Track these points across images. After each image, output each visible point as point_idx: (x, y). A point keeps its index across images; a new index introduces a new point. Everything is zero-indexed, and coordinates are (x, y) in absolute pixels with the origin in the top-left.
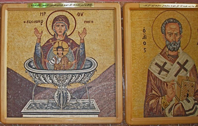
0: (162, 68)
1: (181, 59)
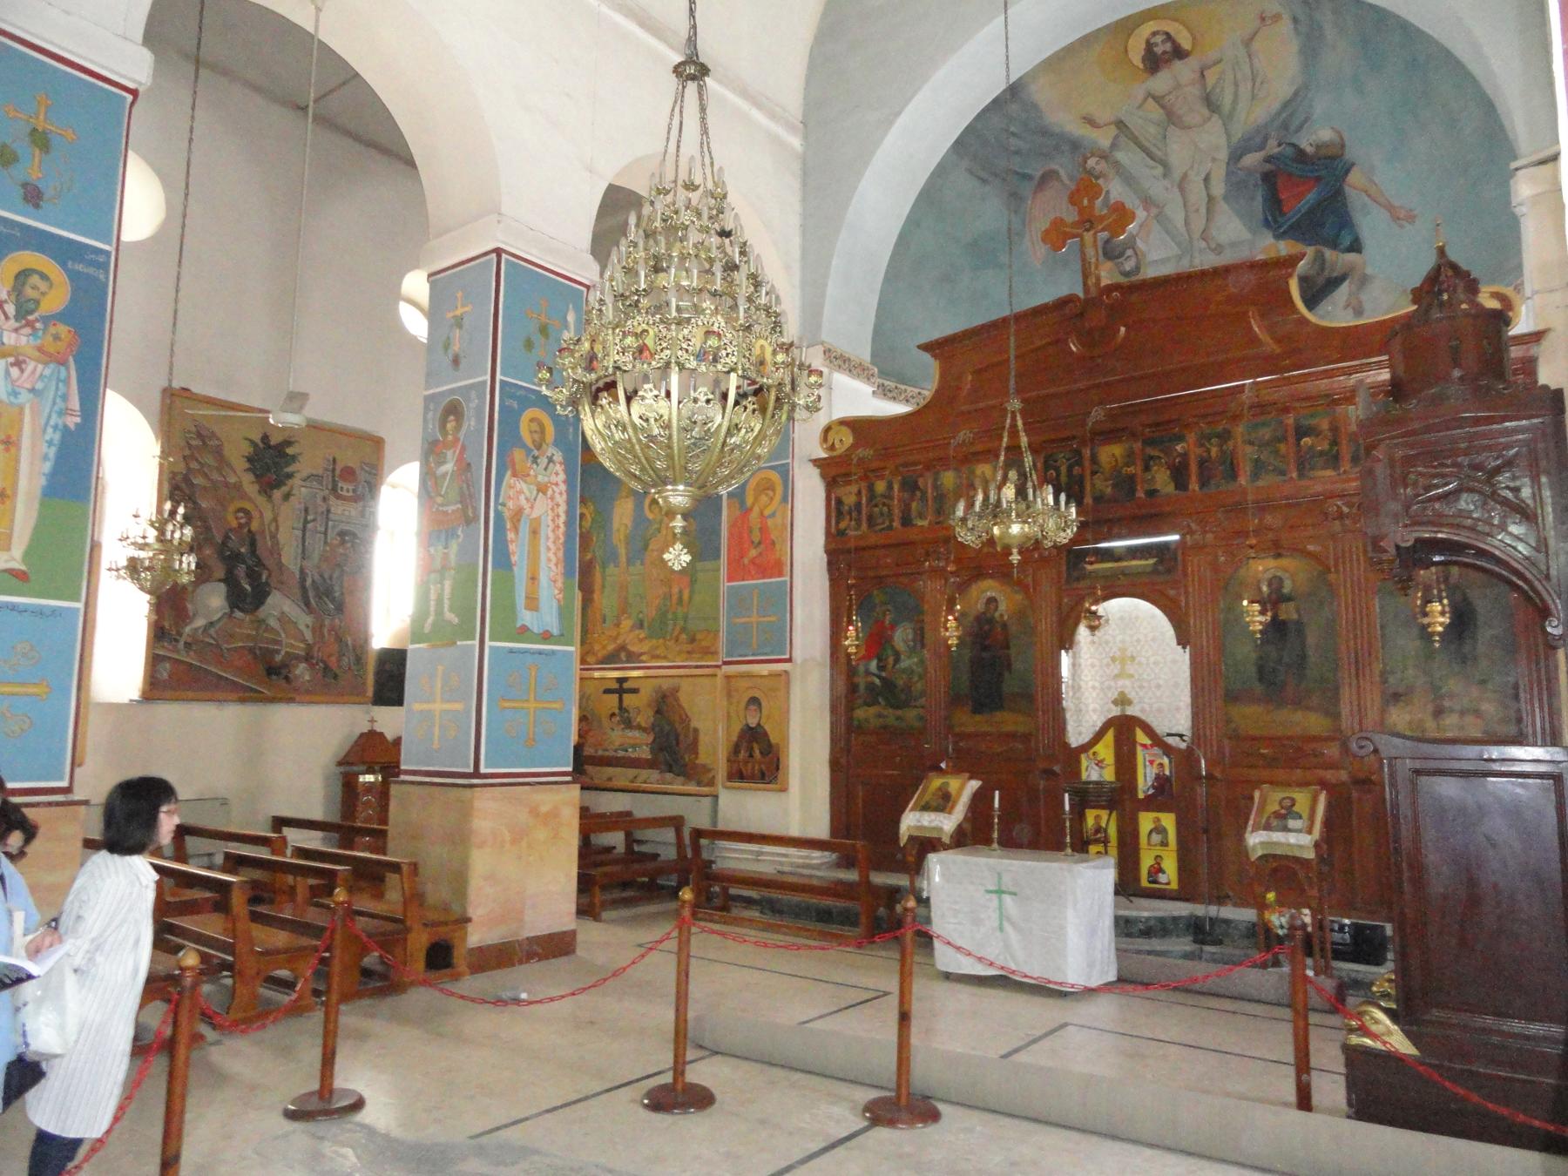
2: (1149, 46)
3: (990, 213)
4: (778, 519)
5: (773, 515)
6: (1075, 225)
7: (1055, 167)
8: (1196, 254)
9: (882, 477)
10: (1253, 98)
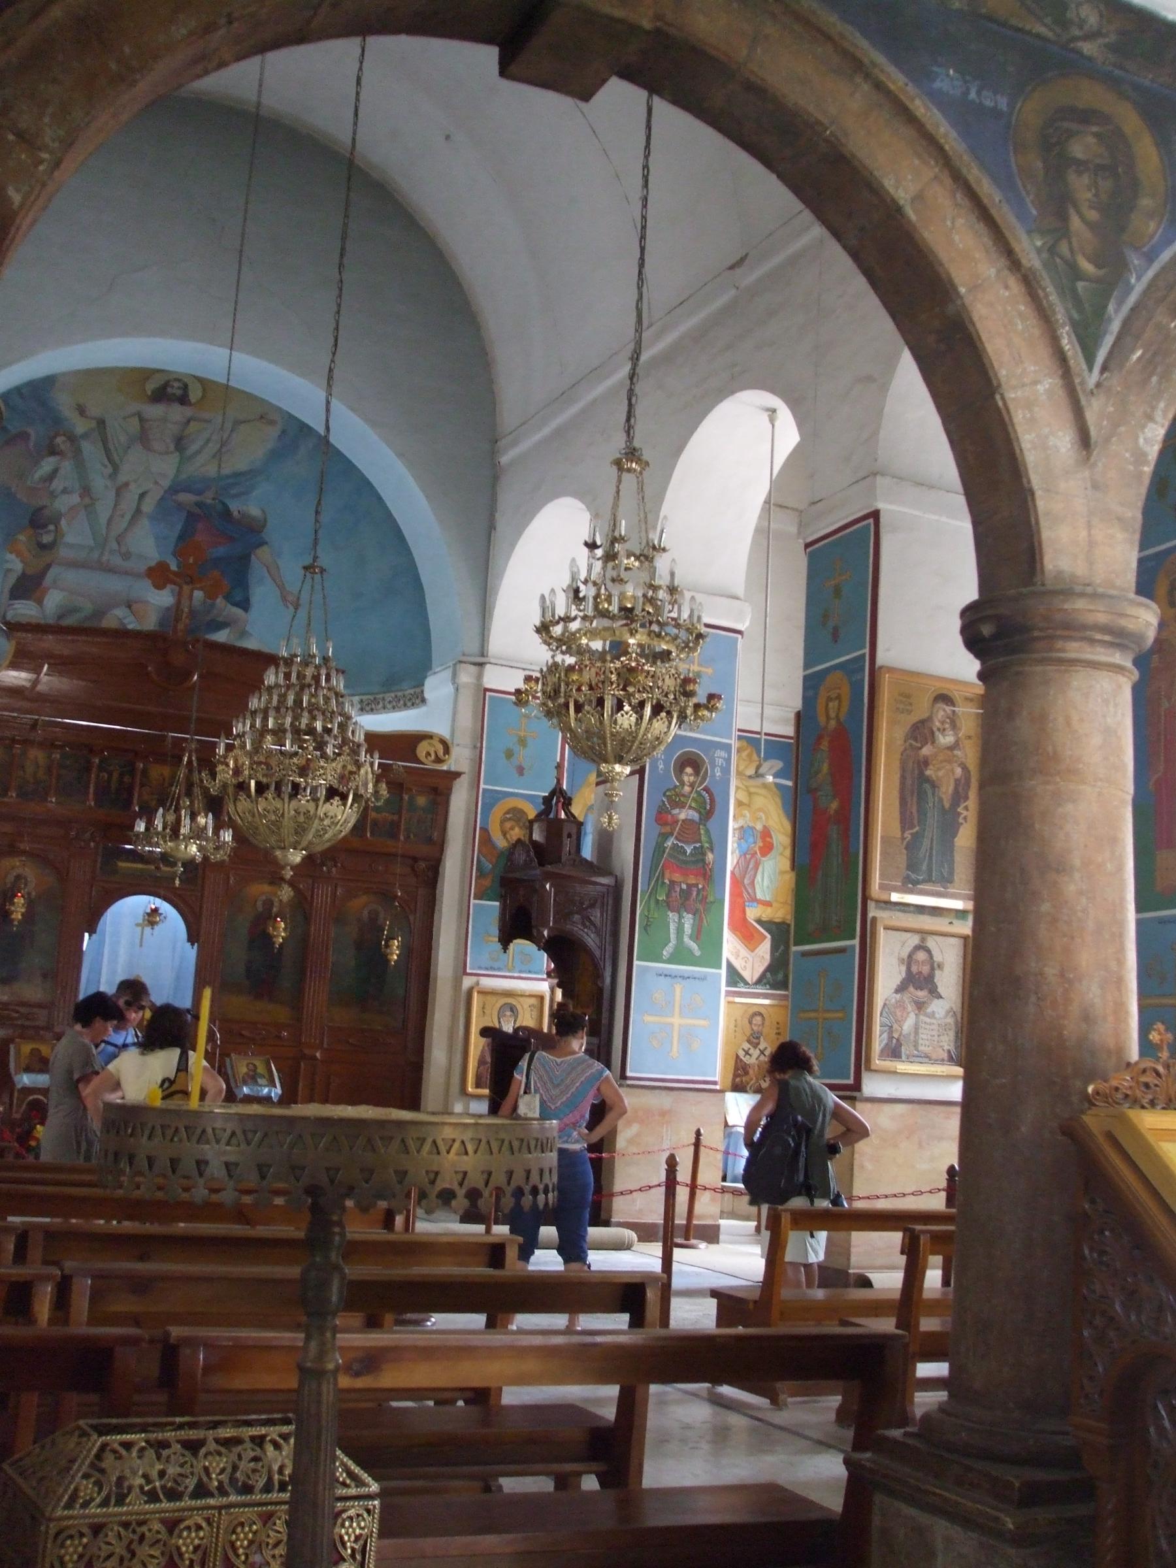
0: (747, 1053)
1: (762, 1047)
2: (166, 385)
6: (175, 573)
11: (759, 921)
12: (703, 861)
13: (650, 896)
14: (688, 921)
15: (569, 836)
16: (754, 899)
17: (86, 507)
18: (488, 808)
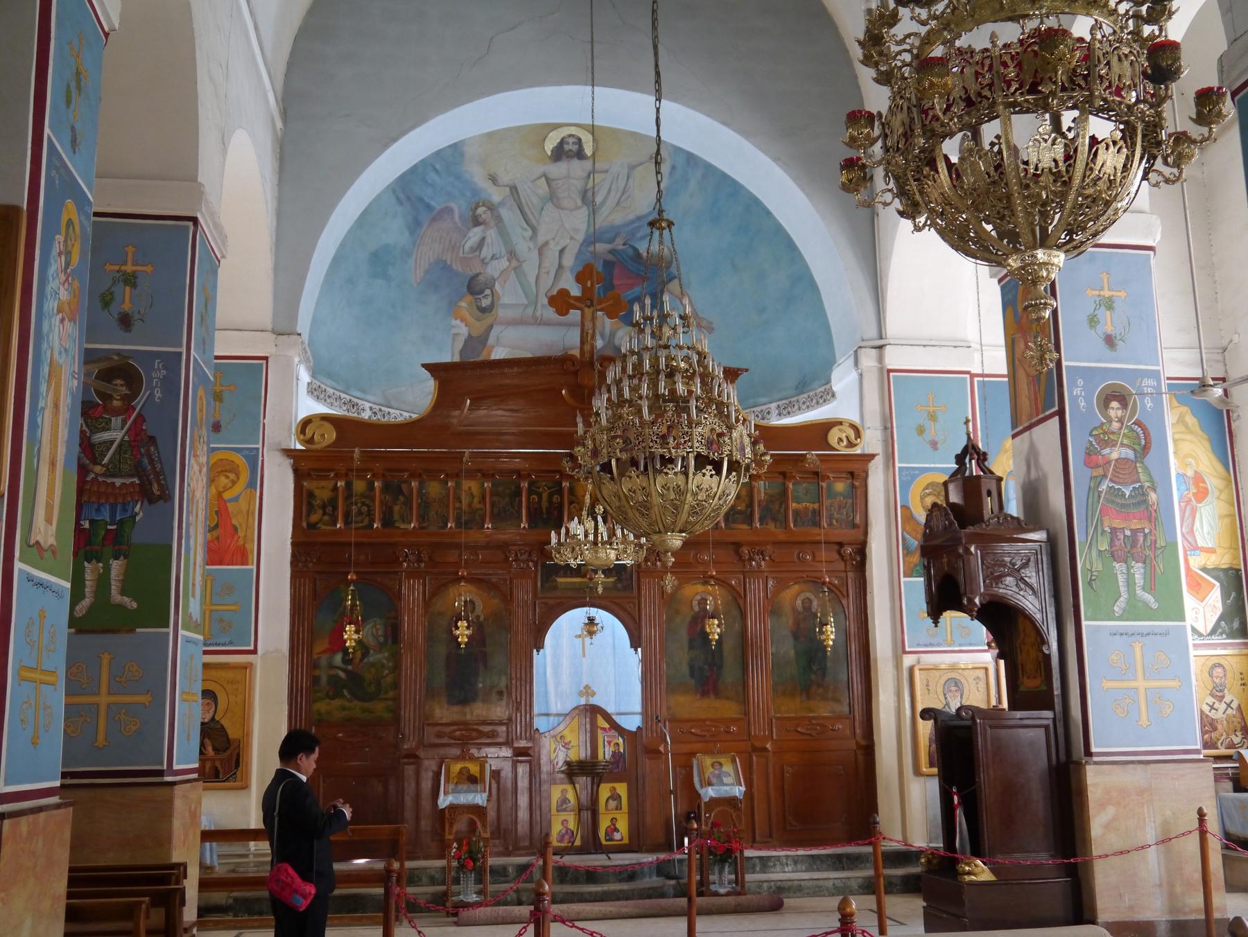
0: (1212, 707)
1: (1227, 699)
2: (562, 142)
3: (394, 232)
4: (243, 504)
5: (236, 499)
6: (576, 298)
7: (453, 205)
8: (539, 307)
9: (364, 478)
10: (617, 204)
11: (1204, 569)
12: (1145, 501)
13: (1090, 548)
14: (1138, 570)
15: (989, 493)
16: (1195, 548)
17: (515, 269)
18: (906, 486)
